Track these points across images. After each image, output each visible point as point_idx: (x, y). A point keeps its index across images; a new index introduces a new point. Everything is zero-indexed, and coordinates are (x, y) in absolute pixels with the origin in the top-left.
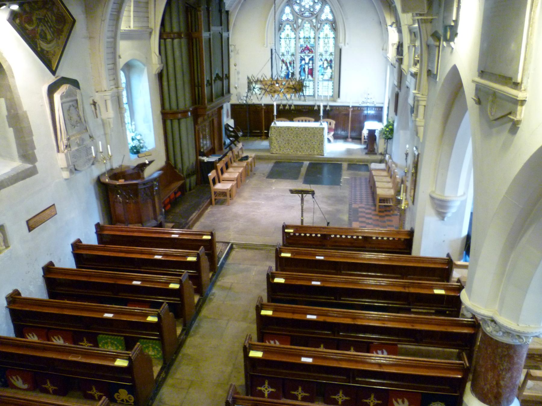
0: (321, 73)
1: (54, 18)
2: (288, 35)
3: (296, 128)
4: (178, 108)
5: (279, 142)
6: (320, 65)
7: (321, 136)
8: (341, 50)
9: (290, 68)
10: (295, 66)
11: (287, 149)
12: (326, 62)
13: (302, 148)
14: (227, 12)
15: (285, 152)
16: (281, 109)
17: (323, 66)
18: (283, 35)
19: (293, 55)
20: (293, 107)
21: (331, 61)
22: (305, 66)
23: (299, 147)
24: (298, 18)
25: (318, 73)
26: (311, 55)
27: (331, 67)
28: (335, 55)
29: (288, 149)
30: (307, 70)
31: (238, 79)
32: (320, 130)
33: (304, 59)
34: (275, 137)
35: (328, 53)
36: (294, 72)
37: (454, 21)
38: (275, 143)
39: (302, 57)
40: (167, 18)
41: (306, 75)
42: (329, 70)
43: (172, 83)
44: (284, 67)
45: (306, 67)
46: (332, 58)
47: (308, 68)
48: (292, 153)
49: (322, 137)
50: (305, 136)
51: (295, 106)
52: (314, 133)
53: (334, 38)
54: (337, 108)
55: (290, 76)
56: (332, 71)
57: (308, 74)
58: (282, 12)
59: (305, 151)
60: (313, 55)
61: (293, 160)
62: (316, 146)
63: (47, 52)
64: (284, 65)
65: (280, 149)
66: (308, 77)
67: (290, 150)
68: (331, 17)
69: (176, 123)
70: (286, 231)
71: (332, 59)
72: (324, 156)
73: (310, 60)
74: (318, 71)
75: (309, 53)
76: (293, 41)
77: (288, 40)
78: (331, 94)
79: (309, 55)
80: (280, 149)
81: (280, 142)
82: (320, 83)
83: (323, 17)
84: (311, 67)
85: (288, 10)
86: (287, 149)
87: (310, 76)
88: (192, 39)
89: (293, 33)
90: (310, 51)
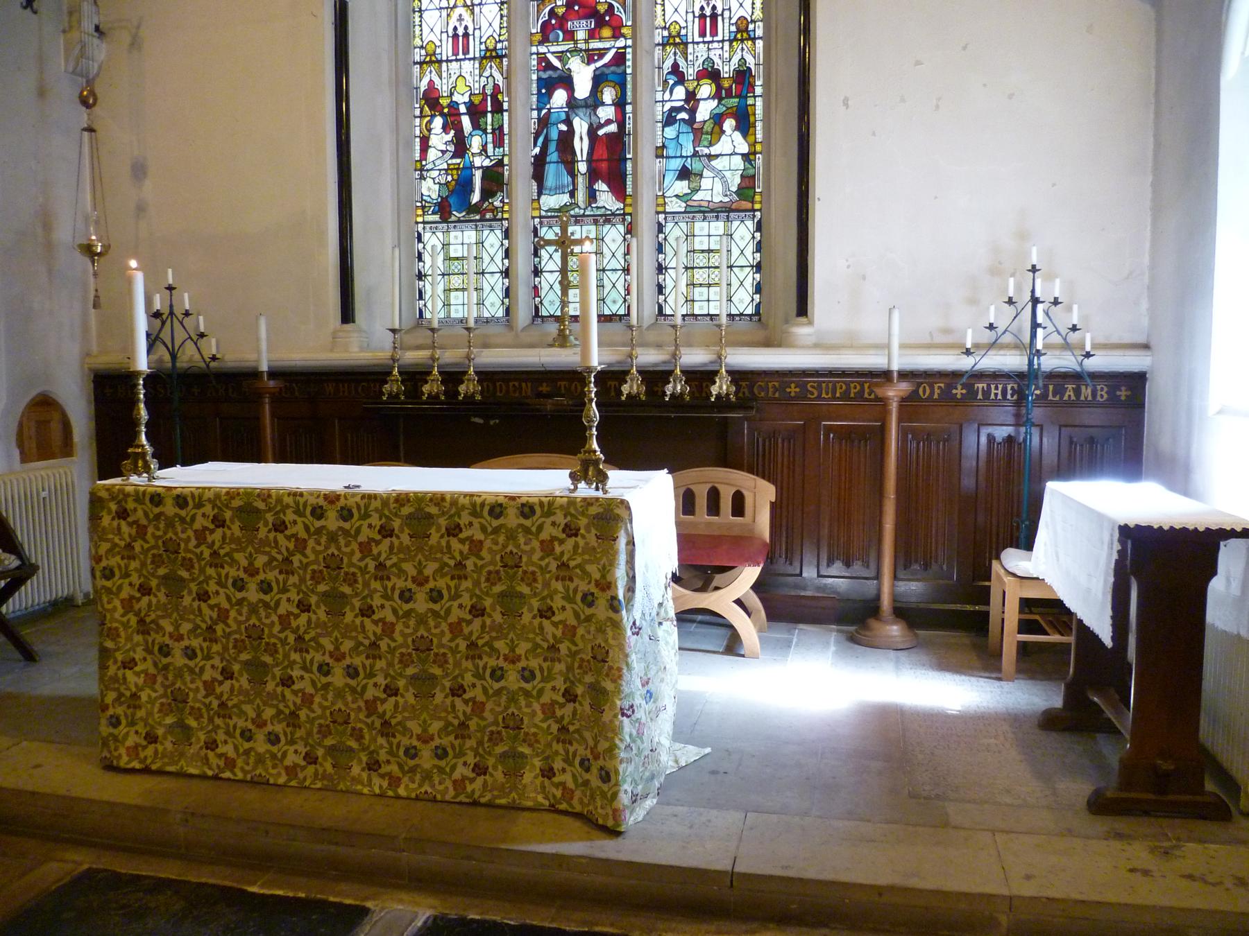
0: (676, 164)
3: (318, 513)
5: (165, 651)
6: (668, 106)
7: (589, 600)
9: (476, 143)
10: (506, 130)
11: (247, 735)
12: (706, 89)
13: (387, 729)
15: (230, 764)
16: (393, 397)
17: (693, 112)
19: (491, 56)
21: (743, 76)
22: (568, 122)
23: (359, 719)
25: (659, 164)
26: (609, 45)
27: (745, 125)
28: (766, 38)
29: (260, 736)
30: (581, 146)
31: (141, 209)
32: (571, 531)
33: (566, 81)
34: (128, 604)
35: (724, 29)
36: (500, 163)
38: (129, 664)
39: (550, 66)
41: (581, 181)
42: (732, 141)
44: (440, 140)
45: (580, 126)
46: (752, 56)
47: (592, 132)
48: (292, 771)
49: (601, 610)
50: (421, 604)
51: (488, 377)
52: (511, 563)
54: (793, 390)
55: (476, 197)
56: (753, 145)
57: (593, 176)
59: (426, 759)
60: (621, 43)
61: (263, 862)
62: (534, 718)
64: (438, 122)
65: (183, 731)
66: (592, 196)
67: (273, 739)
71: (751, 61)
72: (614, 833)
74: (660, 152)
75: (592, 35)
78: (744, 301)
79: (595, 44)
80: (183, 731)
81: (179, 660)
82: (674, 232)
84: (613, 128)
86: (247, 735)
87: (601, 186)
90: (601, 23)
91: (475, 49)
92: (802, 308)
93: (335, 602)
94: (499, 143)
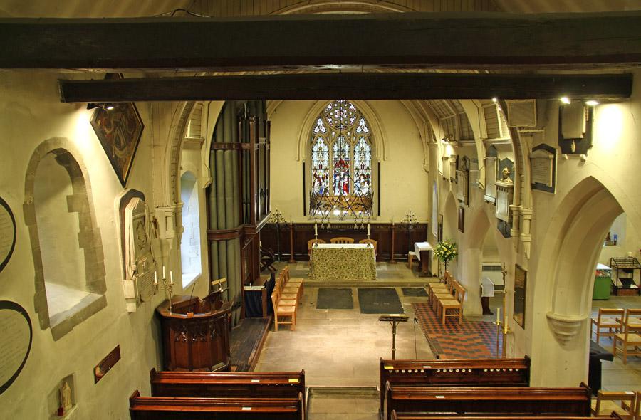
1: (127, 123)
2: (320, 148)
4: (226, 228)
8: (379, 164)
9: (323, 184)
12: (362, 177)
14: (269, 122)
18: (315, 149)
19: (326, 169)
20: (329, 227)
21: (368, 175)
24: (331, 131)
27: (368, 183)
37: (583, 134)
40: (219, 126)
42: (366, 185)
43: (221, 198)
44: (317, 183)
47: (344, 183)
51: (331, 225)
53: (370, 151)
57: (344, 190)
58: (315, 125)
63: (120, 159)
68: (366, 130)
69: (223, 244)
70: (385, 368)
73: (344, 175)
76: (326, 156)
77: (320, 154)
83: (359, 130)
85: (320, 122)
88: (242, 151)
89: (326, 147)
91: (323, 168)
92: (379, 215)
93: (342, 260)
94: (327, 182)
